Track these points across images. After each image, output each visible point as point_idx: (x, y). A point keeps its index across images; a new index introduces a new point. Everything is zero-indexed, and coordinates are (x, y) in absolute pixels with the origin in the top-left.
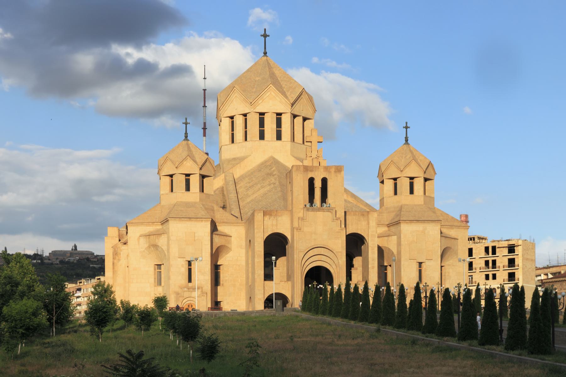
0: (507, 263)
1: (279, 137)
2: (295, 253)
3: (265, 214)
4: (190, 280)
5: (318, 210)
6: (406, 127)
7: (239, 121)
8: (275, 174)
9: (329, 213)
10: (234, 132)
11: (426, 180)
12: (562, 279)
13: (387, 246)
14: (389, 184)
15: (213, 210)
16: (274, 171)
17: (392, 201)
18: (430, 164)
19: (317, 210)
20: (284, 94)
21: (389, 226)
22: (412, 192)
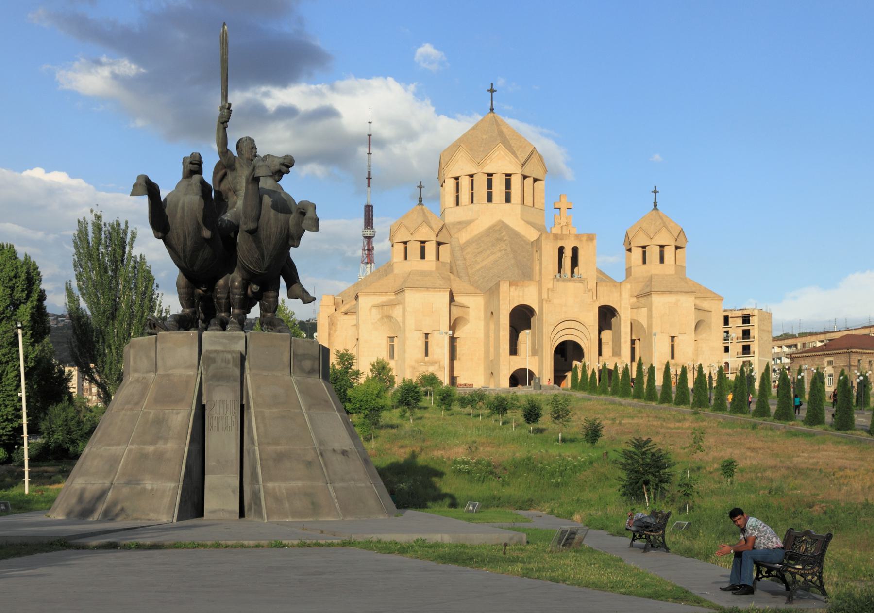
0: (741, 335)
1: (508, 200)
2: (544, 327)
3: (511, 285)
4: (427, 354)
5: (569, 281)
6: (655, 192)
7: (465, 183)
8: (506, 240)
9: (580, 284)
10: (460, 194)
11: (677, 248)
12: (813, 354)
14: (637, 253)
15: (449, 279)
16: (504, 236)
17: (639, 270)
18: (682, 231)
20: (514, 153)
21: (638, 297)
22: (662, 260)
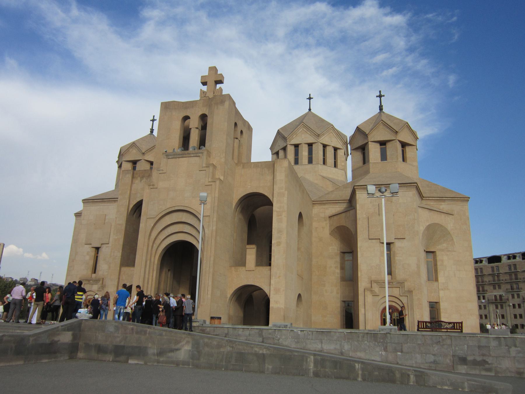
1: (310, 161)
4: (95, 271)
7: (281, 153)
9: (197, 159)
11: (404, 145)
13: (345, 225)
19: (180, 156)
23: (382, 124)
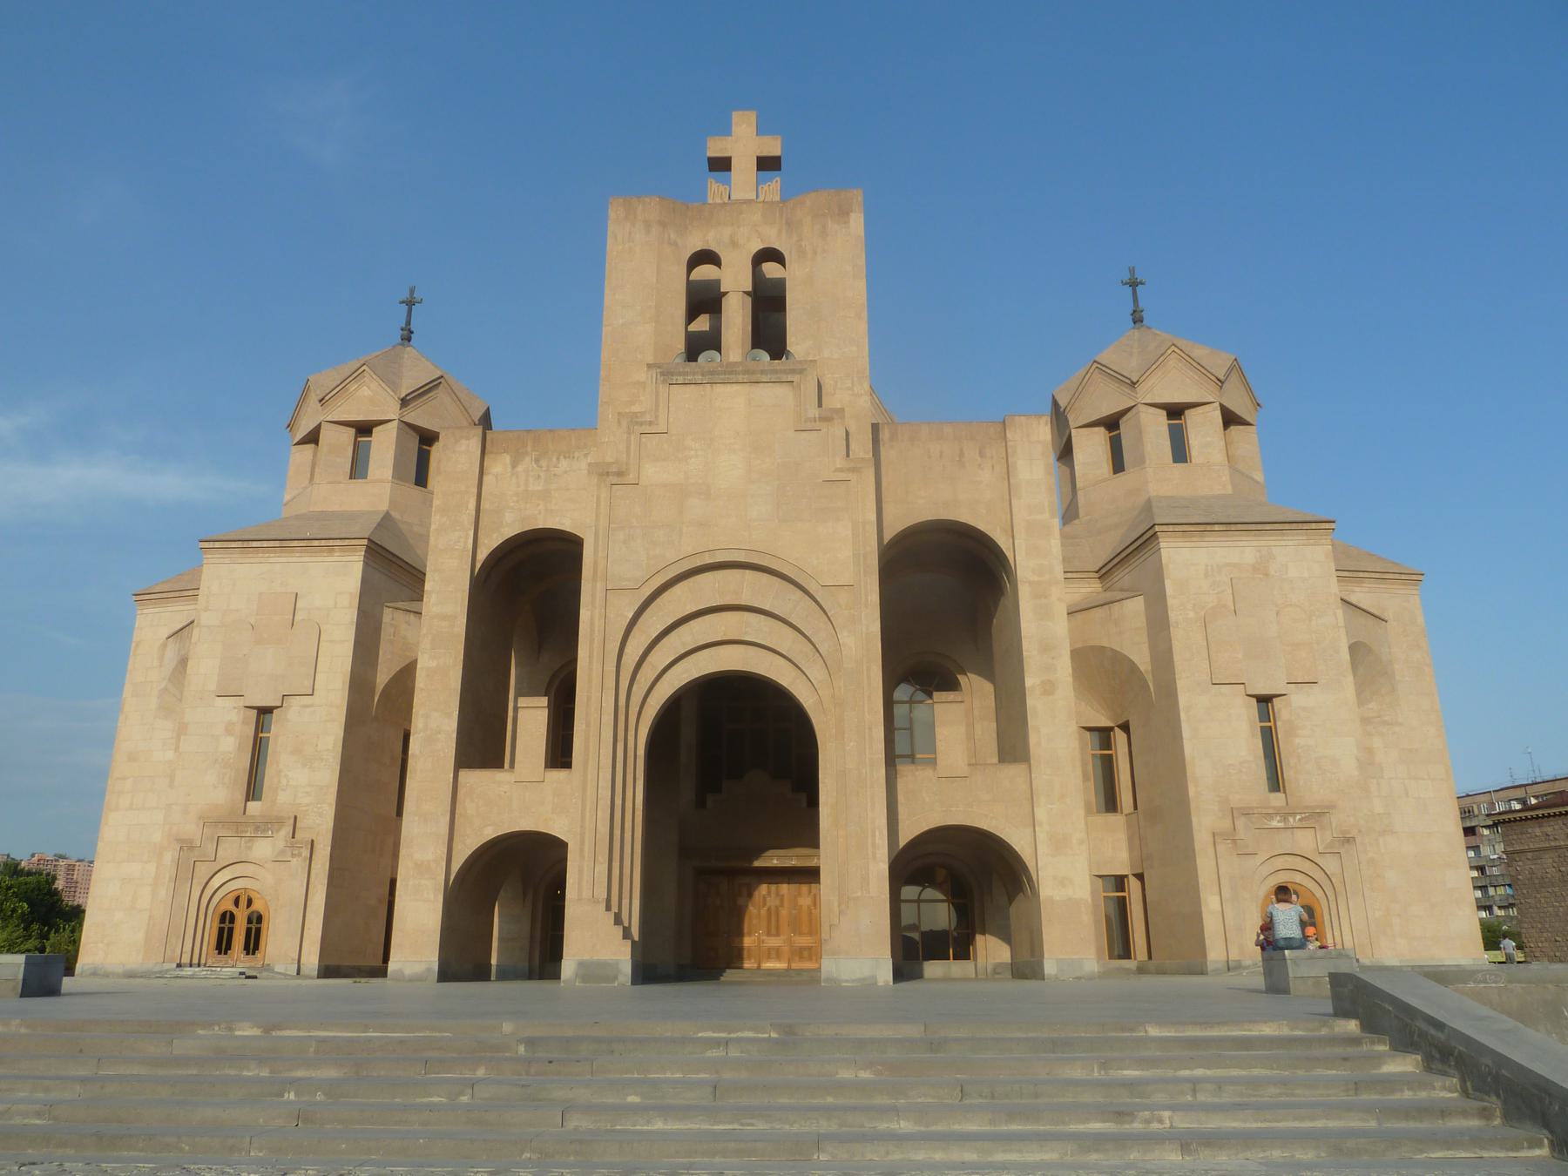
11: (1230, 419)
13: (1105, 644)
21: (1105, 573)
22: (1180, 453)
23: (1174, 355)
